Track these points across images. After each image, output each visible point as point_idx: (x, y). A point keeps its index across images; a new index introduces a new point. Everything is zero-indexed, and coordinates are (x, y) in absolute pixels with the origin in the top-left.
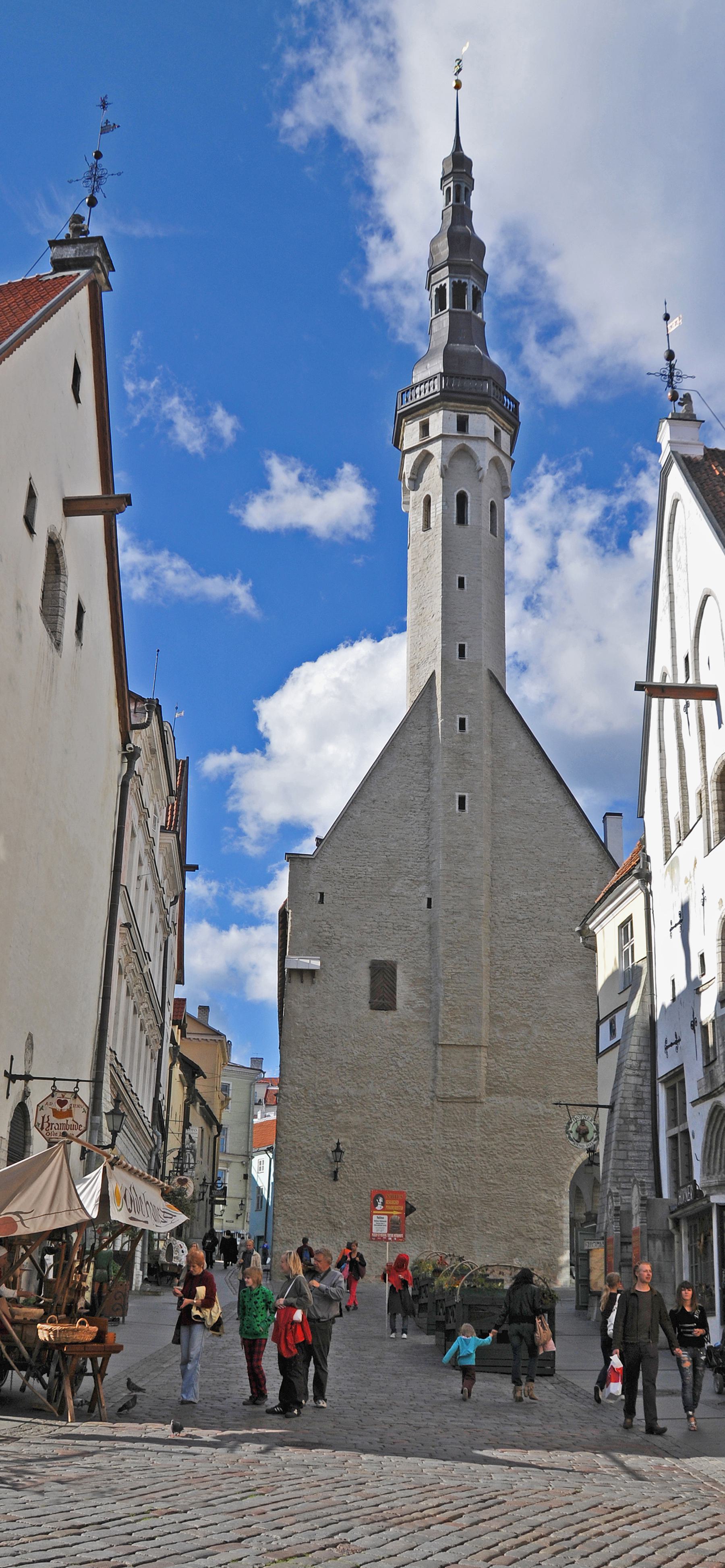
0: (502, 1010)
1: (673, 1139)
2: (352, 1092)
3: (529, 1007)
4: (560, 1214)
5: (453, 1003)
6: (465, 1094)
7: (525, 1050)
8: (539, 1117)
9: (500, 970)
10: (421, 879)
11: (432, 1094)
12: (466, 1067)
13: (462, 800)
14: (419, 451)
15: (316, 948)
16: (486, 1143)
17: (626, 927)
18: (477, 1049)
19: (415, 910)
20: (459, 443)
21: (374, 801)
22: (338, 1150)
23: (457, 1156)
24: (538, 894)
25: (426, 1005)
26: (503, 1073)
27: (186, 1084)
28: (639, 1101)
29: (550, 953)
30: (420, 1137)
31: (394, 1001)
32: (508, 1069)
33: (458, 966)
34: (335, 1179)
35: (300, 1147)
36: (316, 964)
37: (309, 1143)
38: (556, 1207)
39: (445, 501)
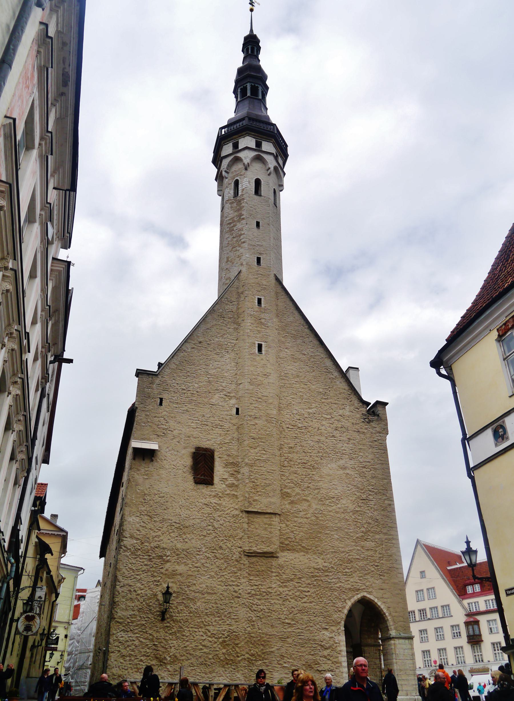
0: (290, 488)
2: (179, 546)
3: (308, 487)
5: (256, 481)
6: (265, 550)
7: (306, 518)
8: (318, 569)
9: (287, 460)
10: (232, 395)
11: (240, 549)
12: (265, 529)
13: (260, 347)
14: (232, 157)
15: (155, 436)
16: (281, 589)
18: (273, 516)
21: (200, 342)
23: (259, 599)
24: (310, 411)
25: (235, 482)
26: (292, 535)
27: (39, 553)
29: (320, 451)
30: (231, 583)
32: (295, 532)
33: (259, 454)
34: (163, 619)
35: (135, 591)
36: (154, 446)
37: (142, 587)
38: (336, 643)
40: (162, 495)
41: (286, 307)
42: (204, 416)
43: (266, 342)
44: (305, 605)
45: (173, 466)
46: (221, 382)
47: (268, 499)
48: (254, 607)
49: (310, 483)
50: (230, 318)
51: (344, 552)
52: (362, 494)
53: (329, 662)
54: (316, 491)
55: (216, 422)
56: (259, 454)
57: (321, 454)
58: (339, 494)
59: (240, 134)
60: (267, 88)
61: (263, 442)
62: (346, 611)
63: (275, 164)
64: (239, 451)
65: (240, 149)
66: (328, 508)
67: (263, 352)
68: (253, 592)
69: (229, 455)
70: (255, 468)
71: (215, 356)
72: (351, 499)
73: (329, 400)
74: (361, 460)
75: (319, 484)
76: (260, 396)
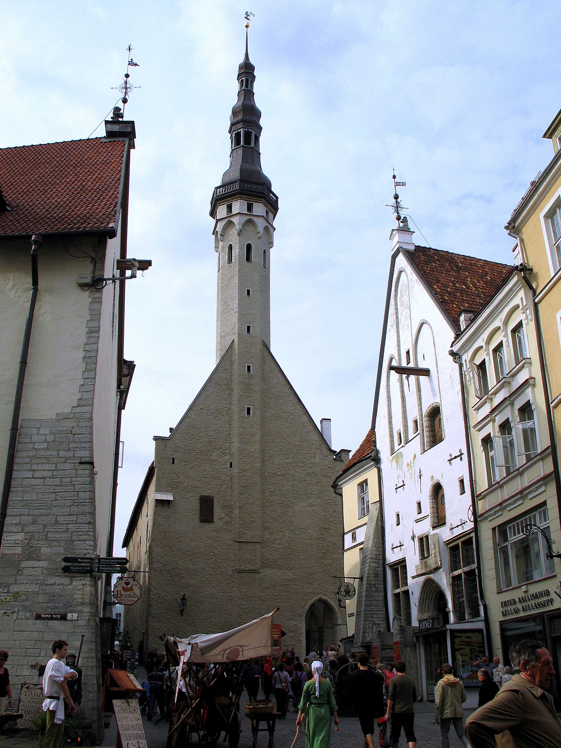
1: (397, 596)
2: (190, 567)
3: (284, 521)
4: (300, 632)
6: (251, 568)
10: (226, 452)
13: (249, 409)
14: (226, 221)
16: (261, 594)
17: (363, 485)
20: (248, 217)
22: (184, 599)
24: (288, 461)
28: (376, 575)
31: (212, 517)
33: (246, 499)
34: (182, 615)
35: (162, 597)
36: (171, 498)
39: (241, 248)
40: (177, 532)
44: (278, 604)
48: (243, 606)
50: (225, 385)
51: (308, 567)
53: (293, 640)
54: (290, 524)
56: (246, 499)
59: (233, 197)
60: (260, 128)
62: (307, 608)
63: (266, 224)
67: (251, 414)
68: (242, 596)
69: (225, 500)
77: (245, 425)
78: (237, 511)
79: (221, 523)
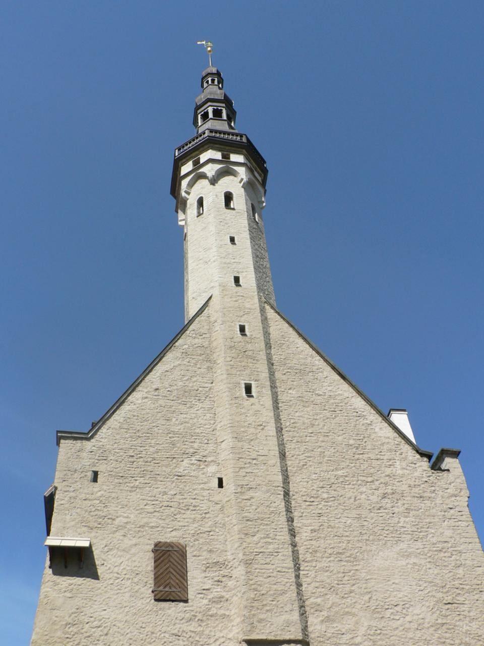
10: (209, 459)
15: (85, 529)
19: (203, 489)
21: (157, 389)
24: (340, 473)
25: (224, 594)
29: (364, 532)
40: (96, 623)
41: (283, 336)
42: (165, 493)
43: (256, 381)
45: (116, 575)
46: (192, 442)
47: (283, 617)
49: (354, 585)
50: (201, 355)
52: (444, 595)
55: (185, 501)
57: (365, 537)
58: (406, 599)
61: (267, 524)
64: (227, 543)
65: (201, 162)
66: (391, 623)
69: (211, 551)
70: (256, 566)
71: (180, 407)
72: (427, 604)
73: (365, 456)
74: (434, 540)
75: (369, 585)
76: (254, 456)
77: (243, 411)
78: (239, 572)
79: (205, 602)
